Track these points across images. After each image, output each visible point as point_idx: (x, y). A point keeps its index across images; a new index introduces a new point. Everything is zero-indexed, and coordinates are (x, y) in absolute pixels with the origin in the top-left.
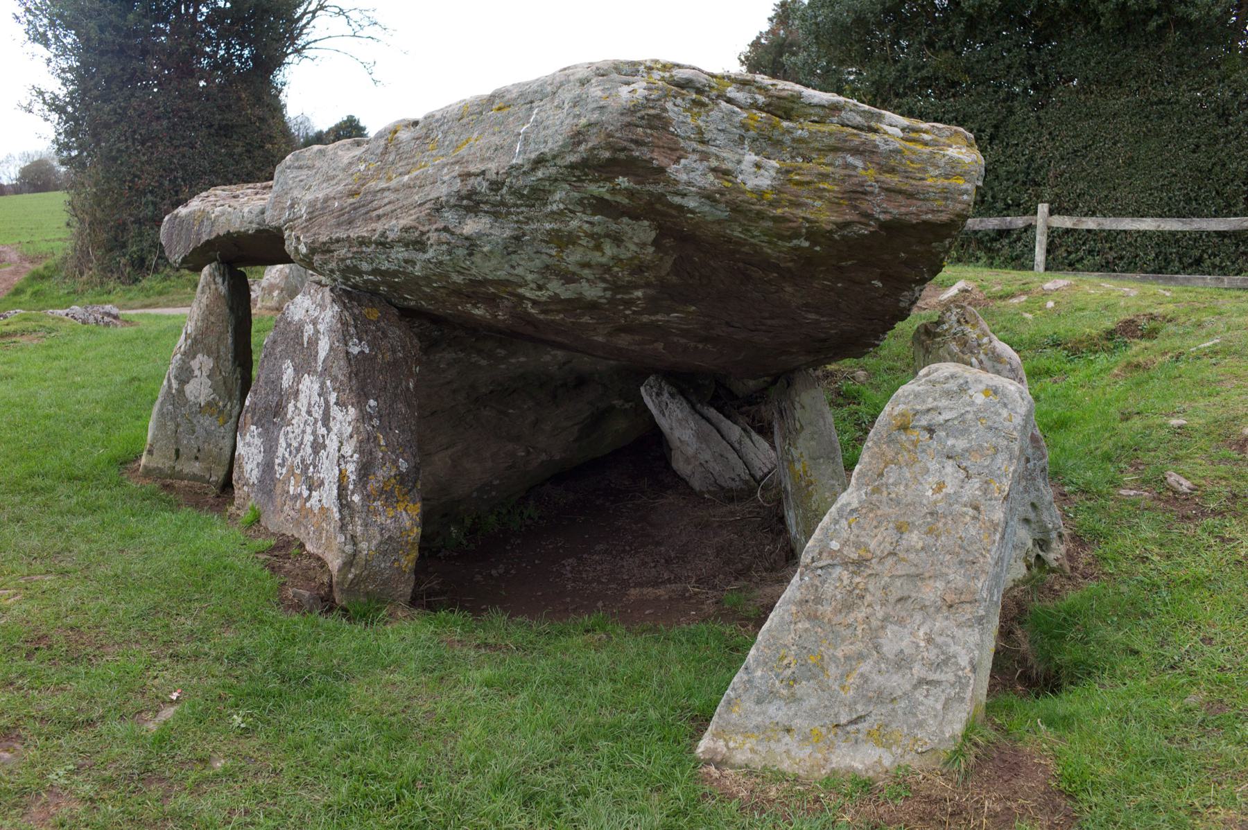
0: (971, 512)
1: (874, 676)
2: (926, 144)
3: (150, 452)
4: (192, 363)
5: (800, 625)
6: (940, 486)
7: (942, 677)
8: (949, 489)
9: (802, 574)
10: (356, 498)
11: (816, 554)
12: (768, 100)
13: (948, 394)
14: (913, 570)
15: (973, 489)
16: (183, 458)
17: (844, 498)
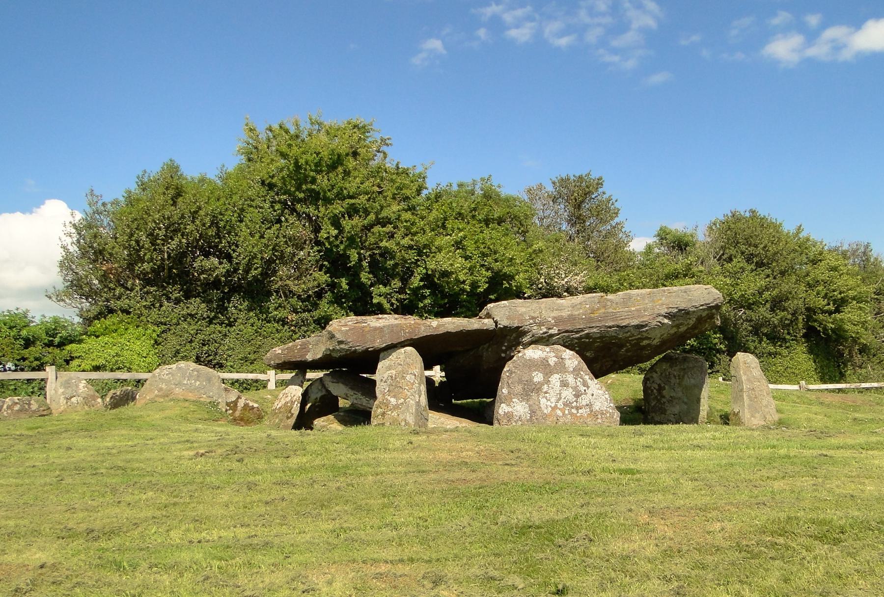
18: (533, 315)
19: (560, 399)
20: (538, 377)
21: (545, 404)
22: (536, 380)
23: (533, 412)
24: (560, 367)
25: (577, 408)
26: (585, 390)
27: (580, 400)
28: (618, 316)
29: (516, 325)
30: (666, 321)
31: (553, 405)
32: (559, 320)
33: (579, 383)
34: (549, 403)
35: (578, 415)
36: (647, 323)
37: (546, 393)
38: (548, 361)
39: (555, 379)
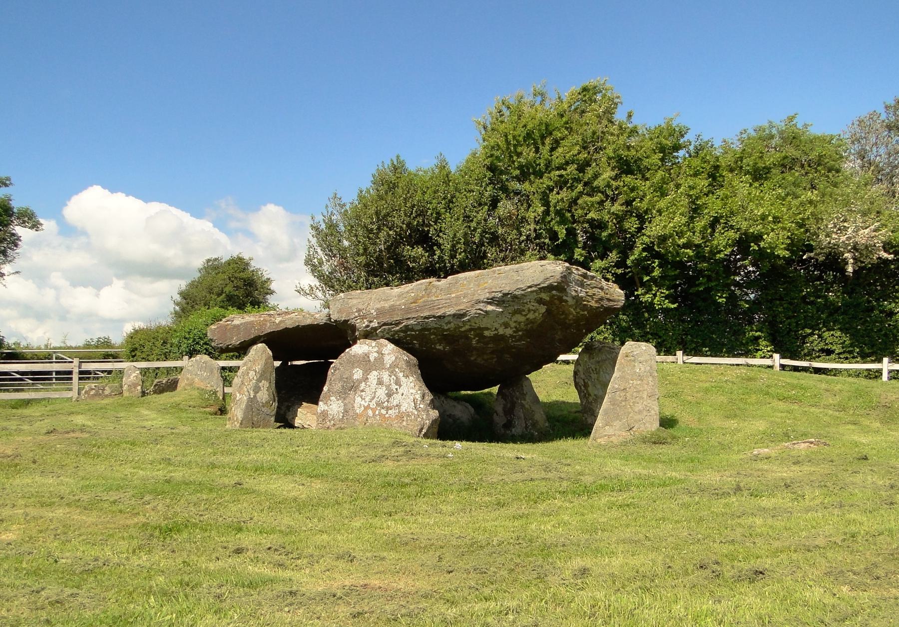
10: (422, 406)
17: (614, 375)
18: (361, 307)
19: (374, 398)
20: (358, 374)
21: (359, 403)
22: (356, 377)
23: (346, 411)
24: (379, 363)
25: (388, 408)
26: (396, 389)
27: (391, 400)
28: (435, 304)
29: (343, 319)
30: (490, 308)
31: (366, 405)
32: (381, 312)
33: (392, 381)
34: (363, 402)
35: (387, 416)
36: (464, 311)
37: (362, 391)
38: (369, 357)
39: (373, 376)
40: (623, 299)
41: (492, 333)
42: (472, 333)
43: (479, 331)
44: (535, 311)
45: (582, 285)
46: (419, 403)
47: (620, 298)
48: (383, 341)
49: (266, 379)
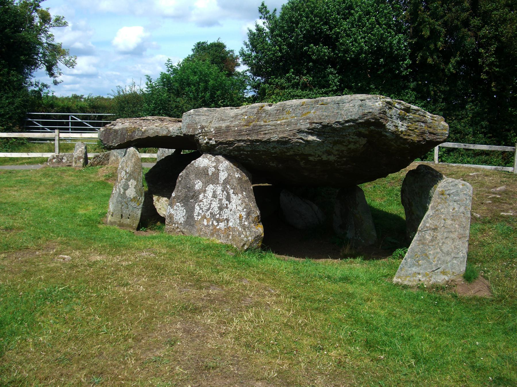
0: (463, 215)
1: (442, 257)
2: (436, 121)
3: (112, 215)
4: (129, 183)
5: (420, 246)
6: (454, 209)
7: (459, 256)
8: (456, 209)
9: (419, 233)
10: (246, 223)
11: (422, 228)
12: (404, 108)
13: (453, 186)
14: (449, 230)
15: (462, 209)
16: (124, 218)
17: (428, 213)
18: (204, 124)
24: (214, 179)
25: (218, 221)
26: (227, 204)
30: (311, 138)
32: (219, 131)
35: (218, 227)
36: (287, 139)
38: (208, 171)
39: (210, 188)
40: (447, 132)
41: (315, 158)
42: (298, 157)
43: (305, 157)
44: (355, 143)
45: (402, 118)
46: (244, 220)
47: (444, 131)
48: (220, 157)
49: (135, 179)
